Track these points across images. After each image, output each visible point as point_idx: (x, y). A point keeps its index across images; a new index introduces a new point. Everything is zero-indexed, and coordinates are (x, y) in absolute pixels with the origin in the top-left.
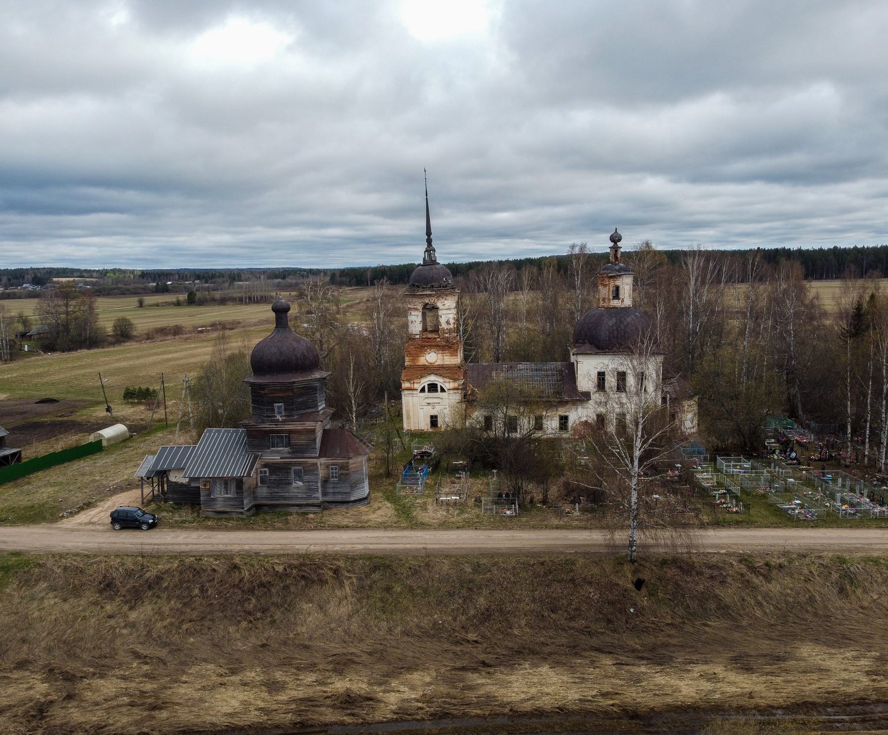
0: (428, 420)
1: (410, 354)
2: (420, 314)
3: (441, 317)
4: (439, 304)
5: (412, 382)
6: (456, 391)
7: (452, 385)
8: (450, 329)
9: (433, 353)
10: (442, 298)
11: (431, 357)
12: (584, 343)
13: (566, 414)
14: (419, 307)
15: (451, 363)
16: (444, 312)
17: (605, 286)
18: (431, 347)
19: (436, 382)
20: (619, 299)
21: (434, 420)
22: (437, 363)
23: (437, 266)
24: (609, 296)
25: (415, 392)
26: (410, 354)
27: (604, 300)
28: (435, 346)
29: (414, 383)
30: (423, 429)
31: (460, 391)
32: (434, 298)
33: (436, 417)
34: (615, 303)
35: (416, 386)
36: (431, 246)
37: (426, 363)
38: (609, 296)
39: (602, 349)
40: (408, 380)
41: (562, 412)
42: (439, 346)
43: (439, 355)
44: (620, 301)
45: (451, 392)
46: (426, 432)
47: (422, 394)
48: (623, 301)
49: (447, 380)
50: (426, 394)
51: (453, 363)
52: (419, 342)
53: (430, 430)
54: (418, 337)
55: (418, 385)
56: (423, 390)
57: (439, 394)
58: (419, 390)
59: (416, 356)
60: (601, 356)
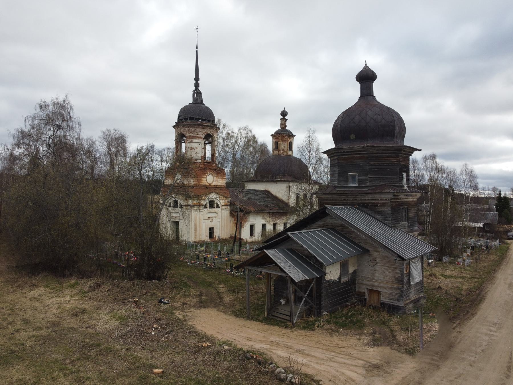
0: (208, 231)
11: (210, 179)
17: (285, 141)
18: (211, 170)
19: (215, 200)
23: (202, 105)
24: (287, 148)
30: (203, 239)
34: (290, 152)
35: (203, 203)
37: (207, 184)
38: (287, 148)
42: (215, 170)
45: (224, 207)
47: (205, 210)
52: (201, 166)
53: (209, 240)
54: (200, 161)
57: (216, 210)
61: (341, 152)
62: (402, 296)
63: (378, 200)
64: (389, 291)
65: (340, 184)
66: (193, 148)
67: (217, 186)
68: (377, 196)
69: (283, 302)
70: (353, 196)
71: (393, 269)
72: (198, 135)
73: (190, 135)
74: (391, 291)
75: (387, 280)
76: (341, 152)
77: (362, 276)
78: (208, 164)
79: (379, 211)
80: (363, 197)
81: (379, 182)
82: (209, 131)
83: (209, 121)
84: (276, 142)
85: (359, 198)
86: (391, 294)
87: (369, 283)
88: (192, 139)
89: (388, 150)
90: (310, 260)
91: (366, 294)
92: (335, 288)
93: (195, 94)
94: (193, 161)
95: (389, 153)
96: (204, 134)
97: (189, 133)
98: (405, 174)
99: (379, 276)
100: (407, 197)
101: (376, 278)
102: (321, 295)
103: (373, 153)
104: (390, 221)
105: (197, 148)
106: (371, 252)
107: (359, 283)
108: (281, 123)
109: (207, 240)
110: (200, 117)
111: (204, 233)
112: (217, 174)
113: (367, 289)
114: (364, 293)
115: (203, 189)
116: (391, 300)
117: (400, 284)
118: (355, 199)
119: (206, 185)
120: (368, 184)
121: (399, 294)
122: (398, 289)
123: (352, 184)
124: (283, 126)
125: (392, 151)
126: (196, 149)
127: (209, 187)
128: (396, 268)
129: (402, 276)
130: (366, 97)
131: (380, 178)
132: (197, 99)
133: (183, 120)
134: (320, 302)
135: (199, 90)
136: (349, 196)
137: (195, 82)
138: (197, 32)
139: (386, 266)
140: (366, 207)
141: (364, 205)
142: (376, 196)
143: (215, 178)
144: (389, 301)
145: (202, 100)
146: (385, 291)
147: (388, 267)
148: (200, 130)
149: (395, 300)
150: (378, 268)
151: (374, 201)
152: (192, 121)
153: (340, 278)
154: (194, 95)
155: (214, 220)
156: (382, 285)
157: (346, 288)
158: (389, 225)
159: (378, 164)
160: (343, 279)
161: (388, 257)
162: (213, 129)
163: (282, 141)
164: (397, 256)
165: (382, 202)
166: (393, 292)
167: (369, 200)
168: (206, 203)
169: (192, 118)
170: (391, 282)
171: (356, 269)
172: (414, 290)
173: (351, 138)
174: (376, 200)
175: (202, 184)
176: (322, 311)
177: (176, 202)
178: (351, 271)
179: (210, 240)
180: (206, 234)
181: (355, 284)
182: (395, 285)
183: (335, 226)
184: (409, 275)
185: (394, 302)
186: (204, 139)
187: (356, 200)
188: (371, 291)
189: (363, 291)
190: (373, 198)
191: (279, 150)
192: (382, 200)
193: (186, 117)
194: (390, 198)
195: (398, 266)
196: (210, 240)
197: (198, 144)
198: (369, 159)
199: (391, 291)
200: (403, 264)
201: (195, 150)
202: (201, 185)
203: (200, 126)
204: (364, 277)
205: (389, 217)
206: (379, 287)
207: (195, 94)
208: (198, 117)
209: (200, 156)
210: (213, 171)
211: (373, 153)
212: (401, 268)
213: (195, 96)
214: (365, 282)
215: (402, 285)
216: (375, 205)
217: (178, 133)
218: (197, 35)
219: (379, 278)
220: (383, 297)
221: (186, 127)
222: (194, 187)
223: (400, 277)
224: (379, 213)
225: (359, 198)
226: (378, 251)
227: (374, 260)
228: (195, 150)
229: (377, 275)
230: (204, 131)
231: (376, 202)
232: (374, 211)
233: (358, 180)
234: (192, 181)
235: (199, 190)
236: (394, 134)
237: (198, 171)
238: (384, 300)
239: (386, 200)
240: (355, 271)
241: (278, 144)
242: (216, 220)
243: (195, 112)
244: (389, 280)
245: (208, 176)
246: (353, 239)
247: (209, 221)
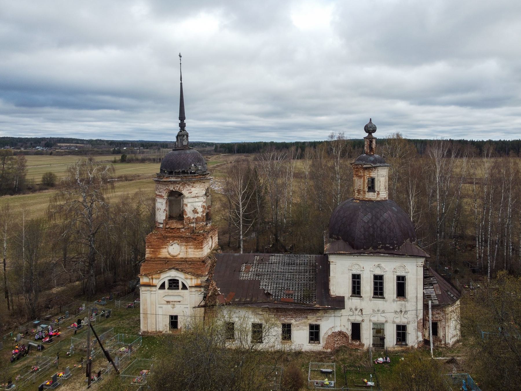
0: (167, 321)
1: (152, 246)
3: (187, 205)
4: (185, 192)
5: (150, 277)
6: (198, 289)
7: (195, 281)
8: (198, 217)
9: (176, 245)
10: (189, 185)
12: (338, 239)
13: (317, 323)
14: (163, 195)
15: (195, 256)
16: (190, 200)
18: (174, 238)
20: (374, 192)
21: (174, 321)
22: (180, 256)
25: (153, 289)
26: (151, 245)
27: (359, 191)
28: (179, 237)
29: (152, 279)
30: (161, 330)
31: (202, 289)
32: (179, 186)
33: (176, 317)
36: (184, 130)
37: (168, 256)
38: (364, 188)
39: (357, 249)
40: (146, 275)
41: (312, 320)
42: (182, 237)
43: (183, 247)
44: (376, 194)
46: (163, 335)
47: (162, 291)
48: (378, 194)
49: (189, 276)
50: (166, 291)
51: (198, 256)
53: (168, 332)
55: (157, 281)
56: (163, 287)
57: (180, 291)
58: (158, 286)
59: (157, 248)
60: (356, 257)
109: (166, 332)
119: (167, 258)
155: (176, 306)
162: (178, 184)
168: (164, 282)
175: (160, 256)
179: (171, 332)
180: (164, 324)
196: (171, 332)
210: (179, 239)
230: (165, 189)
237: (156, 240)
242: (181, 306)
245: (172, 245)
247: (169, 306)
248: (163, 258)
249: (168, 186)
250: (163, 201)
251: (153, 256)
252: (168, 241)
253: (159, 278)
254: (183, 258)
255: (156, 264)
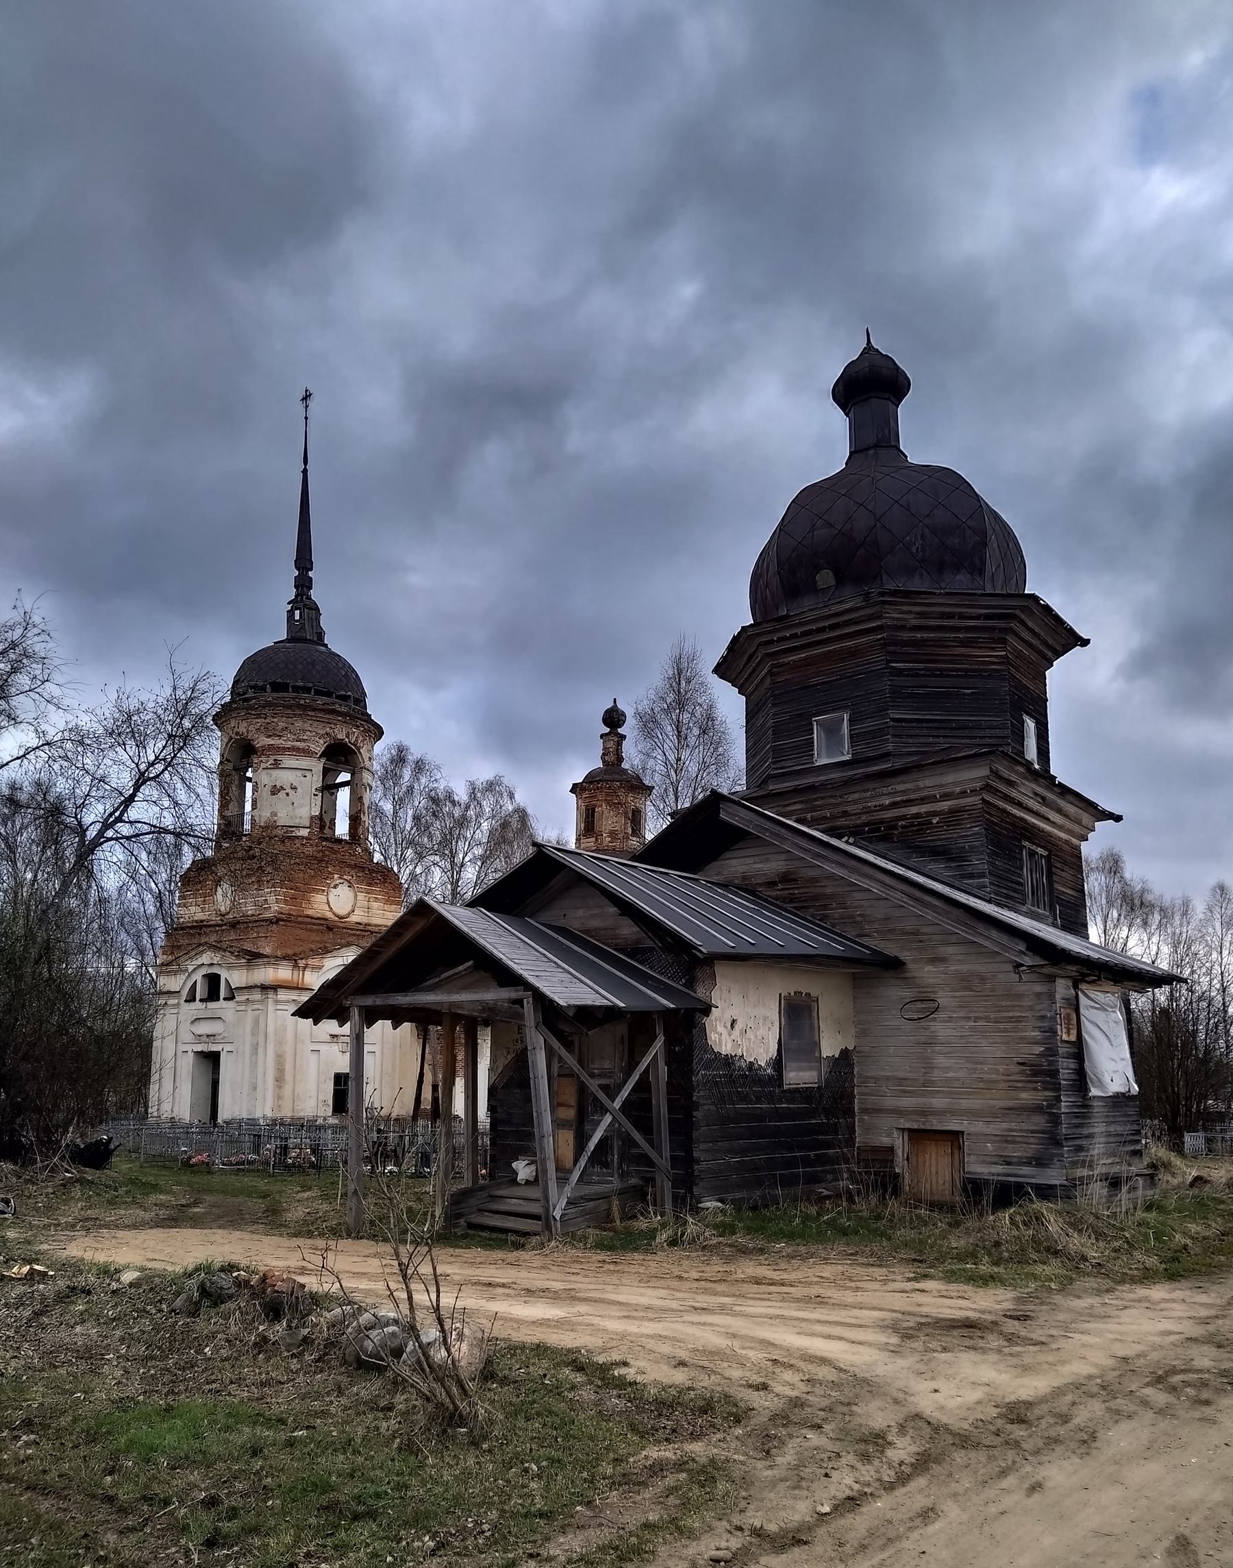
2: (318, 766)
5: (301, 963)
14: (313, 747)
37: (329, 915)
52: (309, 850)
54: (304, 833)
59: (301, 891)
61: (780, 640)
62: (1055, 1141)
63: (932, 799)
64: (1000, 1127)
65: (783, 764)
66: (282, 787)
67: (370, 928)
68: (928, 782)
69: (523, 1169)
70: (833, 801)
71: (1009, 1026)
72: (298, 744)
73: (270, 741)
74: (1005, 1126)
75: (985, 1076)
76: (780, 640)
77: (876, 1079)
78: (336, 847)
79: (939, 843)
80: (872, 797)
81: (931, 739)
82: (341, 733)
83: (345, 698)
84: (587, 810)
85: (855, 802)
86: (1006, 1140)
87: (906, 1102)
88: (279, 758)
89: (962, 617)
90: (641, 964)
91: (900, 1152)
92: (759, 1101)
93: (297, 613)
94: (280, 832)
95: (968, 629)
96: (322, 741)
97: (270, 736)
98: (1030, 725)
99: (947, 1065)
100: (1044, 810)
101: (936, 1075)
102: (689, 1116)
103: (903, 628)
104: (982, 875)
105: (294, 788)
106: (911, 966)
107: (865, 1111)
108: (605, 749)
110: (311, 685)
111: (314, 1094)
112: (369, 885)
113: (903, 1130)
114: (891, 1150)
115: (311, 930)
116: (1008, 1163)
117: (1045, 1089)
118: (841, 809)
120: (890, 747)
121: (1043, 1132)
122: (1038, 1109)
123: (828, 757)
124: (611, 758)
125: (978, 617)
126: (291, 792)
127: (339, 927)
128: (1019, 1020)
129: (1051, 1052)
130: (871, 452)
131: (936, 725)
132: (302, 627)
133: (250, 694)
134: (689, 1151)
135: (309, 598)
136: (816, 799)
137: (297, 573)
138: (307, 407)
139: (976, 1019)
140: (885, 838)
141: (878, 830)
142: (921, 784)
143: (361, 896)
144: (999, 1169)
145: (320, 635)
146: (978, 1127)
147: (987, 1019)
148: (307, 727)
149: (1028, 1164)
150: (941, 1029)
151: (914, 810)
152: (281, 695)
153: (778, 1064)
154: (290, 614)
156: (965, 1104)
157: (810, 1118)
158: (981, 893)
159: (926, 669)
160: (792, 1074)
161: (983, 979)
163: (609, 803)
164: (1022, 947)
165: (946, 805)
166: (1013, 1125)
167: (895, 805)
169: (278, 687)
170: (1003, 1085)
171: (851, 1048)
172: (1103, 1129)
173: (820, 585)
174: (923, 801)
175: (309, 912)
176: (696, 1190)
177: (213, 981)
178: (830, 1047)
180: (322, 1097)
181: (849, 1112)
182: (1024, 1095)
183: (760, 885)
184: (1079, 1050)
185: (1022, 1172)
186: (321, 756)
187: (845, 814)
188: (918, 1136)
189: (885, 1141)
190: (912, 797)
191: (598, 835)
192: (946, 796)
193: (260, 683)
194: (978, 785)
195: (1031, 1008)
197: (299, 773)
198: (892, 649)
199: (1005, 1126)
200: (1051, 996)
201: (287, 794)
202: (307, 916)
203: (305, 710)
204: (888, 1078)
205: (979, 863)
206: (953, 1113)
207: (297, 613)
208: (301, 684)
209: (308, 815)
210: (353, 872)
211: (903, 628)
212: (1043, 1017)
213: (297, 617)
214: (890, 1102)
215: (1050, 1090)
216: (921, 824)
217: (231, 738)
218: (306, 418)
219: (951, 1074)
220: (973, 1159)
221: (258, 716)
222: (278, 920)
223: (1041, 1055)
224: (938, 853)
225: (855, 802)
226: (942, 960)
227: (927, 1006)
228: (287, 794)
229: (941, 1061)
231: (924, 809)
232: (918, 847)
233: (851, 736)
234: (272, 899)
235: (298, 931)
236: (983, 562)
238: (979, 1168)
239: (963, 794)
240: (845, 1053)
241: (593, 816)
243: (291, 667)
244: (994, 1076)
246: (834, 925)
248: (317, 919)
249: (332, 726)
250: (315, 767)
251: (294, 910)
252: (330, 873)
253: (320, 968)
254: (360, 924)
255: (307, 930)
